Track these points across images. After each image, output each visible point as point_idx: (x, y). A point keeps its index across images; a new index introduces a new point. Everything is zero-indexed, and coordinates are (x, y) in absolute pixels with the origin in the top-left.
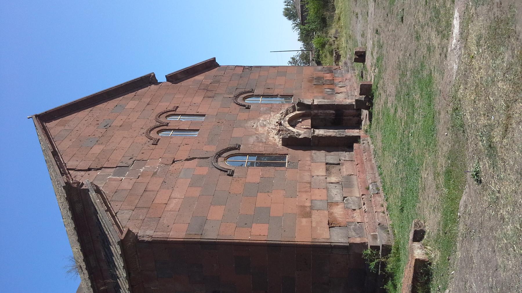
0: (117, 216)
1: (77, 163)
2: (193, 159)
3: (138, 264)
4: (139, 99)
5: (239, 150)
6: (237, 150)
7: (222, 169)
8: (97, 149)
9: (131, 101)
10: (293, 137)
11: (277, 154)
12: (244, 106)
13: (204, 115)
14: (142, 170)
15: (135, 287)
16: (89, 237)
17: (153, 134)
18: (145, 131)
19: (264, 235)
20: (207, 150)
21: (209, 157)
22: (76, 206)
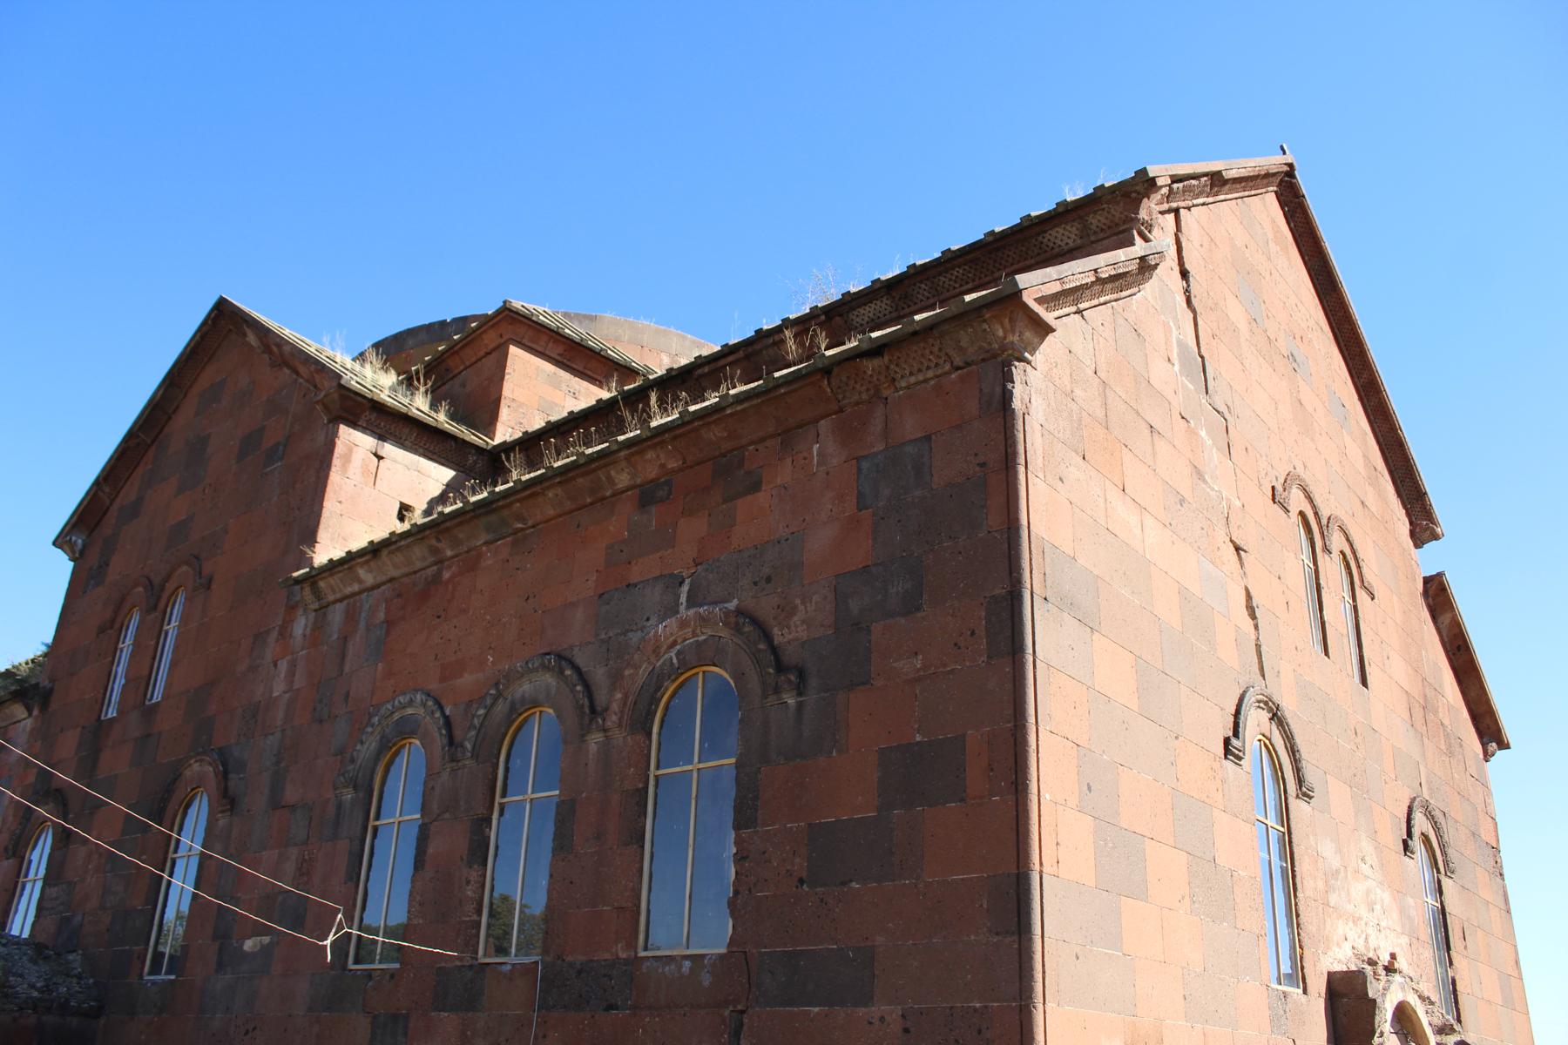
0: (1075, 313)
1: (1197, 244)
2: (1253, 616)
3: (912, 380)
4: (1369, 478)
5: (1297, 797)
6: (1295, 790)
7: (1242, 718)
8: (1237, 314)
9: (1361, 454)
10: (1373, 1015)
11: (1301, 947)
13: (1364, 682)
14: (1203, 433)
15: (826, 382)
16: (955, 288)
18: (1300, 471)
19: (1058, 862)
20: (1282, 675)
21: (1264, 679)
22: (1068, 228)
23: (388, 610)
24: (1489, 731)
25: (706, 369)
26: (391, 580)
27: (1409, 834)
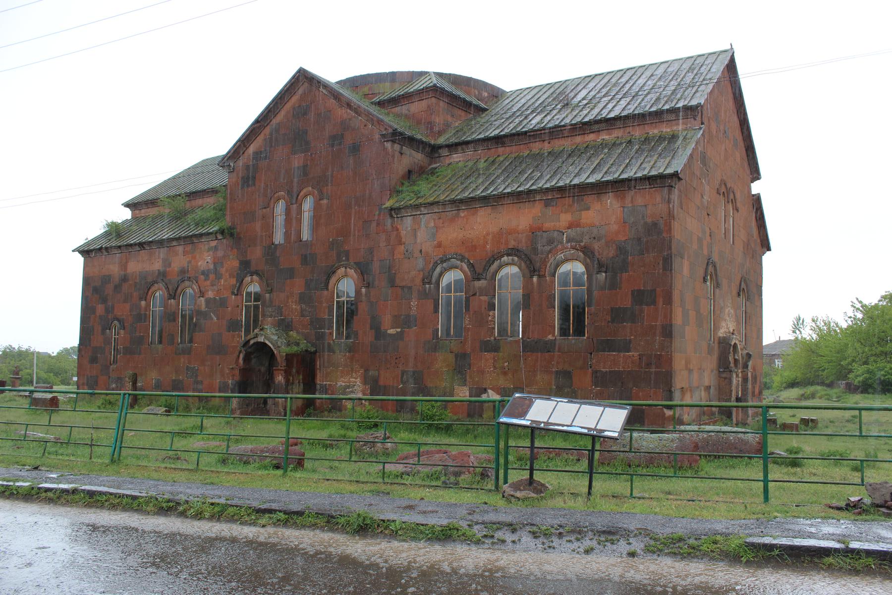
12: (740, 290)
17: (723, 189)
18: (724, 178)
23: (435, 223)
24: (766, 245)
25: (532, 134)
26: (435, 212)
27: (740, 290)
